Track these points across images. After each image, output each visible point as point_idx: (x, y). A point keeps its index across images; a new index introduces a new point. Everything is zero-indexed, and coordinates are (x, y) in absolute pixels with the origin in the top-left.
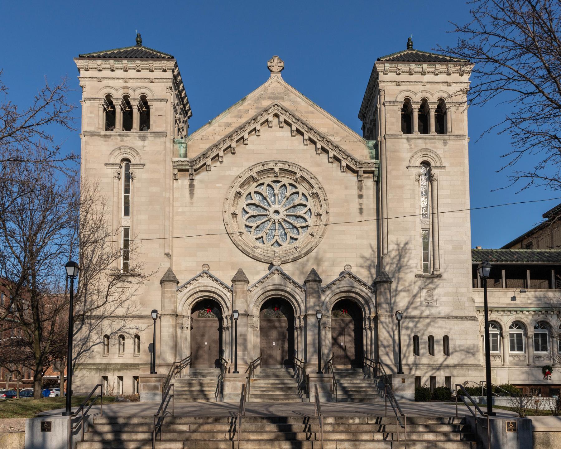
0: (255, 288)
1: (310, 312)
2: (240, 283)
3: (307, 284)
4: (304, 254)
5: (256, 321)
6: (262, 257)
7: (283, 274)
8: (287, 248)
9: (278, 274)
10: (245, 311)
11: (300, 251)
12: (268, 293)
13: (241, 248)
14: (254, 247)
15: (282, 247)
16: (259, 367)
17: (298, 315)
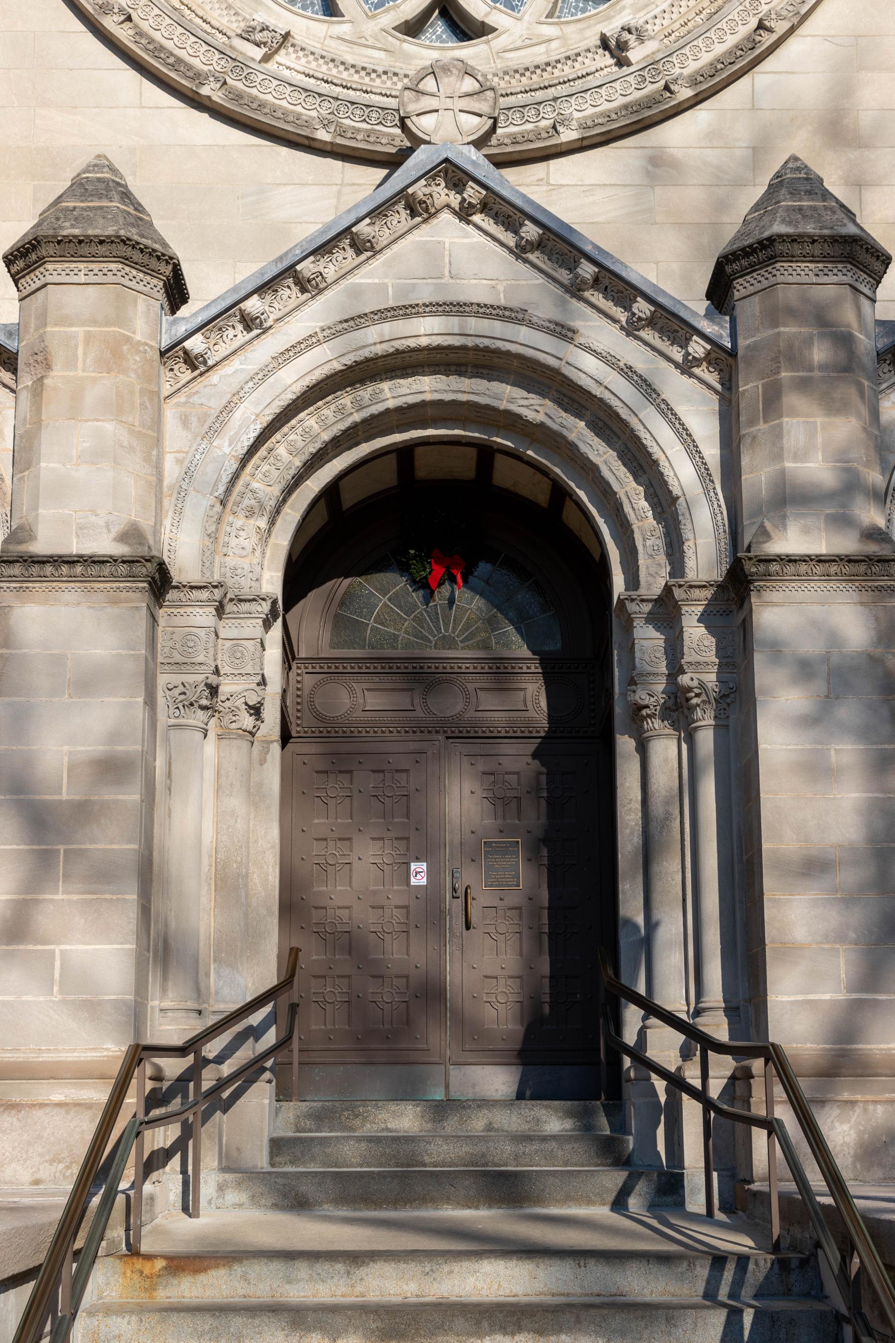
0: (236, 335)
1: (793, 539)
2: (81, 270)
3: (741, 288)
4: (693, 81)
5: (255, 660)
6: (309, 111)
7: (505, 212)
8: (538, 55)
9: (464, 213)
10: (131, 534)
11: (653, 65)
12: (365, 392)
13: (123, 34)
14: (246, 35)
15: (497, 42)
16: (261, 1094)
17: (654, 575)
